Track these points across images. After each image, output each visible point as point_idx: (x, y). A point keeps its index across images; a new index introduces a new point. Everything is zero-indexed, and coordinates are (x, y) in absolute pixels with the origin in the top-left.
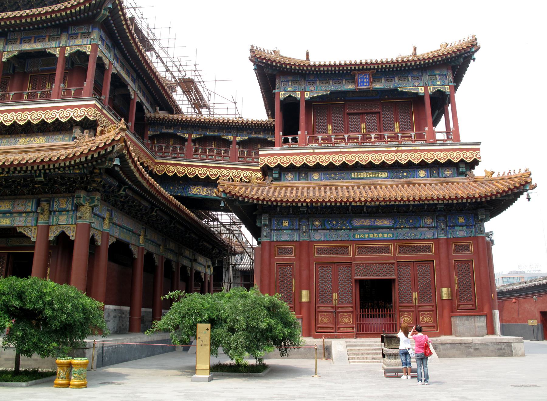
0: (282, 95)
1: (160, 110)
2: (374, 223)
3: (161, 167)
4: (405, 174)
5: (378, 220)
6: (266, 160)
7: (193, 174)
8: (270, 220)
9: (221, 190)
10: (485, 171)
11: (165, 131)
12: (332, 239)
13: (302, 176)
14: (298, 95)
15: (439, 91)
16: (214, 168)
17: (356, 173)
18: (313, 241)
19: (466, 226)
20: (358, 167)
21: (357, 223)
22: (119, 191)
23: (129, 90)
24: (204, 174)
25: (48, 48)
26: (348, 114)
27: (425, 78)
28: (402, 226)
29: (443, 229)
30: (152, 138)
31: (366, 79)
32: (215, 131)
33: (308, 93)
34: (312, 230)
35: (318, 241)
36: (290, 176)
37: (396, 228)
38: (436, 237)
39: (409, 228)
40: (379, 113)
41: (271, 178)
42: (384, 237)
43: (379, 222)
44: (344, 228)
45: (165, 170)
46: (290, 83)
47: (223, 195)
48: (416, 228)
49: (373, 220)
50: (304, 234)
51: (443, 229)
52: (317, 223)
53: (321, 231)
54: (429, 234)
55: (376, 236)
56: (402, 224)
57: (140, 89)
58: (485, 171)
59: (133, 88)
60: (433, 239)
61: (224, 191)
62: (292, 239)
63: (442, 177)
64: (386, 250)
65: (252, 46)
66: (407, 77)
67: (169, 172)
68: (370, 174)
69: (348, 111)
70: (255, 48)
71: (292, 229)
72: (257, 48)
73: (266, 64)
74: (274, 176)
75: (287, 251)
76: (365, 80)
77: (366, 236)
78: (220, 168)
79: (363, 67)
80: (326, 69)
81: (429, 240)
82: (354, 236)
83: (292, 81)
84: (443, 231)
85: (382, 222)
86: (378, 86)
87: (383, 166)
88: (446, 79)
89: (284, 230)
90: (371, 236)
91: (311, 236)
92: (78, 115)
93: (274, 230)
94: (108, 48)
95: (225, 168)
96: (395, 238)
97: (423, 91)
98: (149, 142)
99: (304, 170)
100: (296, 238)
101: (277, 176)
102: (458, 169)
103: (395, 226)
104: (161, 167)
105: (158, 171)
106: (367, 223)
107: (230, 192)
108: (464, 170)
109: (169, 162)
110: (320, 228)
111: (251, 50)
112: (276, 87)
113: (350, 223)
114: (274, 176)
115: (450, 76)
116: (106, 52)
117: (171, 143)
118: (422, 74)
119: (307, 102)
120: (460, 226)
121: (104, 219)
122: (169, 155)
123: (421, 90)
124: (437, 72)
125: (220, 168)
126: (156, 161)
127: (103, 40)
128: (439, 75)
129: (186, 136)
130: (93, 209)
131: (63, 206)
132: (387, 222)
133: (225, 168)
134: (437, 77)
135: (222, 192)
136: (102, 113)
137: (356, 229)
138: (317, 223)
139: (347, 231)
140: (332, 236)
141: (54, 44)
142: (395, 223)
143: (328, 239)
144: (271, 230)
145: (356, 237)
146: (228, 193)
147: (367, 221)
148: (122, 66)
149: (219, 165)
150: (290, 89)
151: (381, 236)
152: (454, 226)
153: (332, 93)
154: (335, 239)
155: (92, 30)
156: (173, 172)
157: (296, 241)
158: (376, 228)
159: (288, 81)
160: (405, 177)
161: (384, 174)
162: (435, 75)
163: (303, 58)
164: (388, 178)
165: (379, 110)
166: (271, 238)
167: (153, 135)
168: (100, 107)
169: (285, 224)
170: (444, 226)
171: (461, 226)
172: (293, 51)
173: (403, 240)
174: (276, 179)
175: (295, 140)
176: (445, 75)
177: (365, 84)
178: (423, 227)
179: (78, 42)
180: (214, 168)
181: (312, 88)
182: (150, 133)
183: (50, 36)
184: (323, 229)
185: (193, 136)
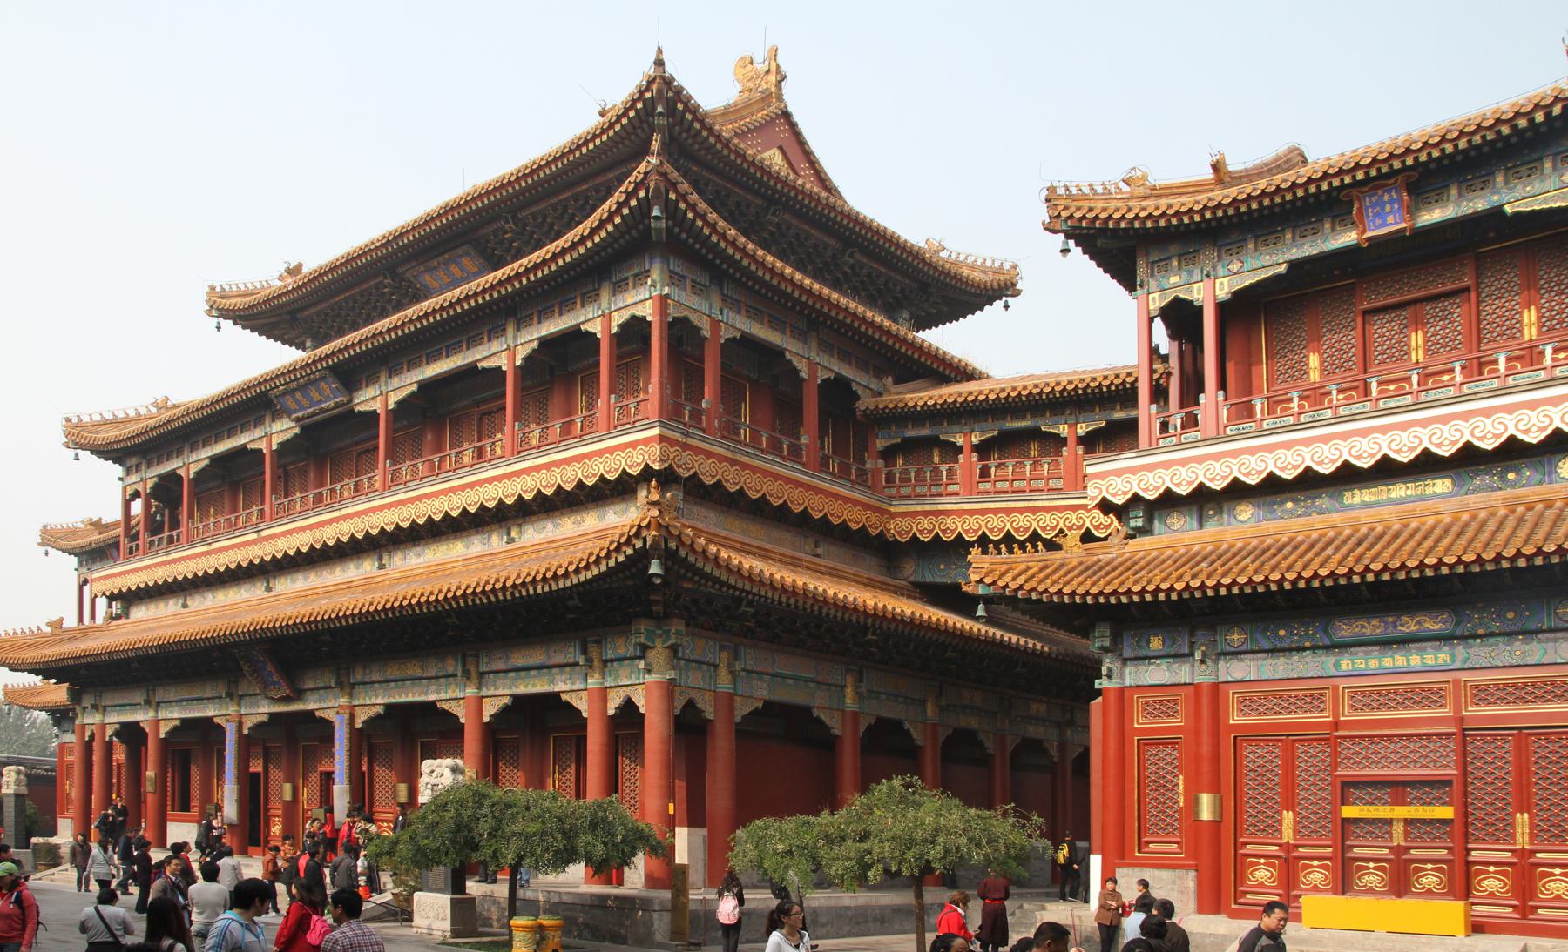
1: (897, 382)
2: (1395, 626)
3: (903, 524)
5: (1405, 619)
7: (976, 531)
9: (975, 578)
11: (911, 433)
16: (1021, 511)
21: (1345, 630)
24: (1001, 530)
28: (1481, 631)
30: (888, 455)
32: (1024, 418)
43: (1409, 626)
47: (981, 591)
56: (1480, 625)
61: (981, 581)
65: (1052, 189)
67: (921, 532)
70: (1061, 191)
78: (1034, 510)
85: (1419, 623)
92: (634, 461)
95: (1047, 509)
96: (1458, 665)
98: (881, 463)
99: (1203, 501)
103: (1458, 633)
104: (903, 524)
105: (899, 533)
106: (1372, 628)
109: (919, 508)
111: (1048, 200)
114: (1133, 523)
117: (936, 459)
122: (924, 490)
125: (1034, 510)
126: (892, 509)
132: (1433, 625)
133: (1047, 509)
142: (1458, 623)
147: (1375, 622)
149: (1031, 504)
156: (930, 532)
158: (1404, 642)
167: (887, 448)
180: (1021, 511)
182: (881, 444)
183: (583, 295)
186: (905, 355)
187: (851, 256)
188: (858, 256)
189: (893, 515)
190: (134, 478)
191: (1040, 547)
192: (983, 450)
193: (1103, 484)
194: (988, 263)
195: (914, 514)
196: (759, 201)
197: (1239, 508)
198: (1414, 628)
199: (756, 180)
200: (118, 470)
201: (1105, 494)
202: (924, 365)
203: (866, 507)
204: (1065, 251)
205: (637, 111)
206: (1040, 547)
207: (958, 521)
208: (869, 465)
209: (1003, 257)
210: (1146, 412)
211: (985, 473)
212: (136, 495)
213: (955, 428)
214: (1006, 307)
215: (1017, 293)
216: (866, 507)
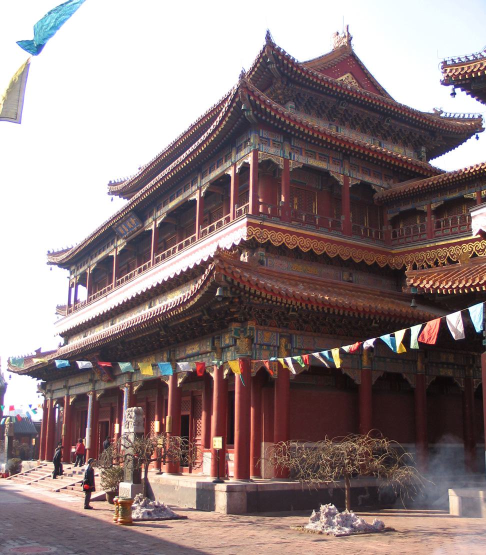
11: (403, 208)
22: (288, 313)
23: (333, 177)
25: (225, 170)
30: (395, 222)
45: (404, 262)
57: (353, 167)
59: (338, 172)
72: (453, 60)
73: (471, 78)
94: (276, 144)
98: (390, 228)
109: (406, 249)
116: (272, 150)
121: (279, 347)
126: (393, 252)
127: (269, 139)
129: (425, 208)
130: (252, 340)
131: (227, 342)
136: (262, 227)
141: (229, 164)
148: (311, 155)
149: (458, 240)
155: (250, 136)
168: (258, 222)
179: (242, 154)
182: (389, 217)
185: (433, 207)
186: (402, 168)
187: (388, 122)
188: (393, 121)
189: (394, 255)
190: (73, 276)
192: (438, 212)
194: (466, 116)
195: (403, 253)
196: (334, 100)
199: (327, 89)
200: (66, 273)
202: (410, 171)
203: (377, 251)
204: (454, 94)
205: (261, 63)
207: (424, 254)
208: (384, 229)
209: (474, 112)
211: (438, 226)
212: (73, 286)
213: (423, 203)
214: (477, 138)
215: (482, 130)
216: (377, 251)
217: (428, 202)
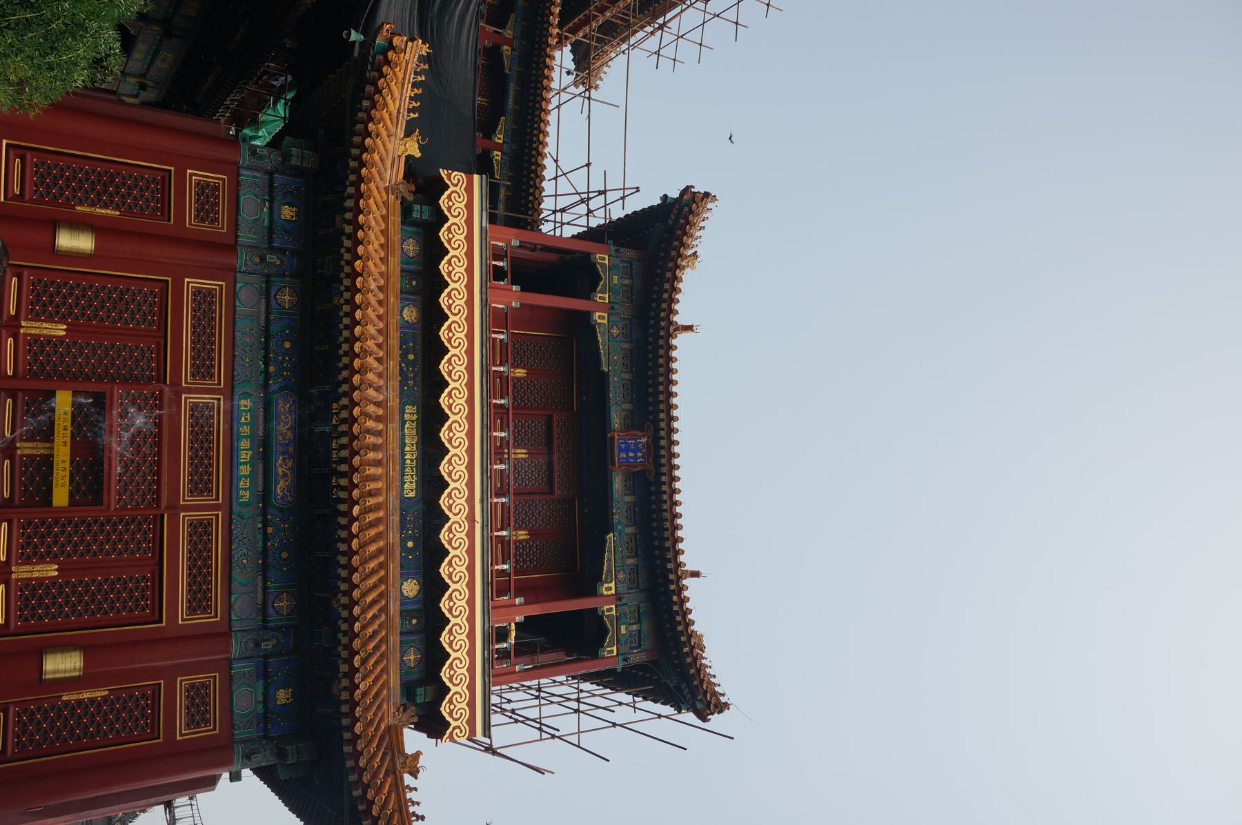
0: (602, 259)
2: (283, 453)
4: (410, 544)
5: (290, 463)
6: (457, 189)
8: (298, 172)
9: (396, 41)
10: (418, 754)
12: (238, 335)
13: (411, 280)
14: (602, 297)
15: (606, 631)
17: (415, 417)
18: (235, 282)
19: (265, 713)
20: (433, 418)
21: (285, 409)
26: (550, 418)
27: (632, 600)
28: (270, 530)
29: (258, 645)
31: (635, 458)
32: (515, 103)
33: (605, 321)
34: (268, 282)
35: (233, 295)
36: (411, 247)
37: (264, 514)
38: (237, 627)
39: (265, 549)
40: (551, 492)
41: (410, 198)
42: (239, 479)
43: (282, 466)
44: (272, 369)
46: (626, 282)
48: (264, 569)
49: (291, 449)
50: (257, 260)
51: (258, 645)
52: (287, 298)
53: (263, 308)
54: (243, 607)
55: (245, 456)
58: (418, 754)
60: (230, 620)
61: (391, 47)
62: (242, 225)
63: (401, 642)
64: (201, 484)
66: (637, 556)
68: (411, 453)
69: (556, 418)
71: (271, 229)
74: (417, 207)
75: (206, 209)
76: (631, 454)
77: (246, 430)
79: (663, 447)
80: (661, 361)
81: (229, 608)
82: (246, 395)
83: (631, 287)
84: (251, 645)
85: (285, 475)
86: (617, 483)
87: (433, 484)
88: (631, 648)
89: (271, 208)
90: (245, 444)
91: (249, 278)
93: (271, 182)
96: (236, 509)
97: (605, 593)
99: (426, 282)
100: (245, 237)
101: (416, 215)
102: (421, 682)
103: (270, 510)
107: (388, 62)
108: (419, 700)
110: (273, 303)
112: (622, 250)
113: (282, 389)
114: (417, 207)
115: (637, 658)
118: (641, 591)
119: (587, 315)
120: (265, 695)
123: (608, 588)
124: (646, 626)
128: (639, 631)
134: (634, 627)
135: (391, 42)
137: (267, 405)
138: (286, 298)
139: (261, 378)
140: (247, 335)
142: (281, 510)
143: (239, 323)
144: (271, 174)
145: (243, 402)
146: (386, 57)
147: (290, 435)
150: (615, 278)
151: (245, 470)
152: (265, 679)
153: (603, 378)
154: (238, 342)
157: (237, 236)
159: (631, 278)
160: (403, 542)
161: (410, 489)
162: (639, 622)
163: (679, 319)
164: (403, 500)
165: (557, 492)
166: (248, 168)
169: (287, 212)
170: (267, 646)
171: (267, 698)
172: (696, 295)
173: (231, 534)
174: (406, 210)
175: (498, 274)
176: (640, 645)
177: (623, 455)
178: (265, 588)
181: (615, 331)
184: (268, 314)
191: (412, 115)
192: (493, 54)
193: (461, 189)
197: (415, 310)
198: (280, 470)
201: (452, 189)
206: (412, 115)
210: (512, 239)
217: (516, 43)
